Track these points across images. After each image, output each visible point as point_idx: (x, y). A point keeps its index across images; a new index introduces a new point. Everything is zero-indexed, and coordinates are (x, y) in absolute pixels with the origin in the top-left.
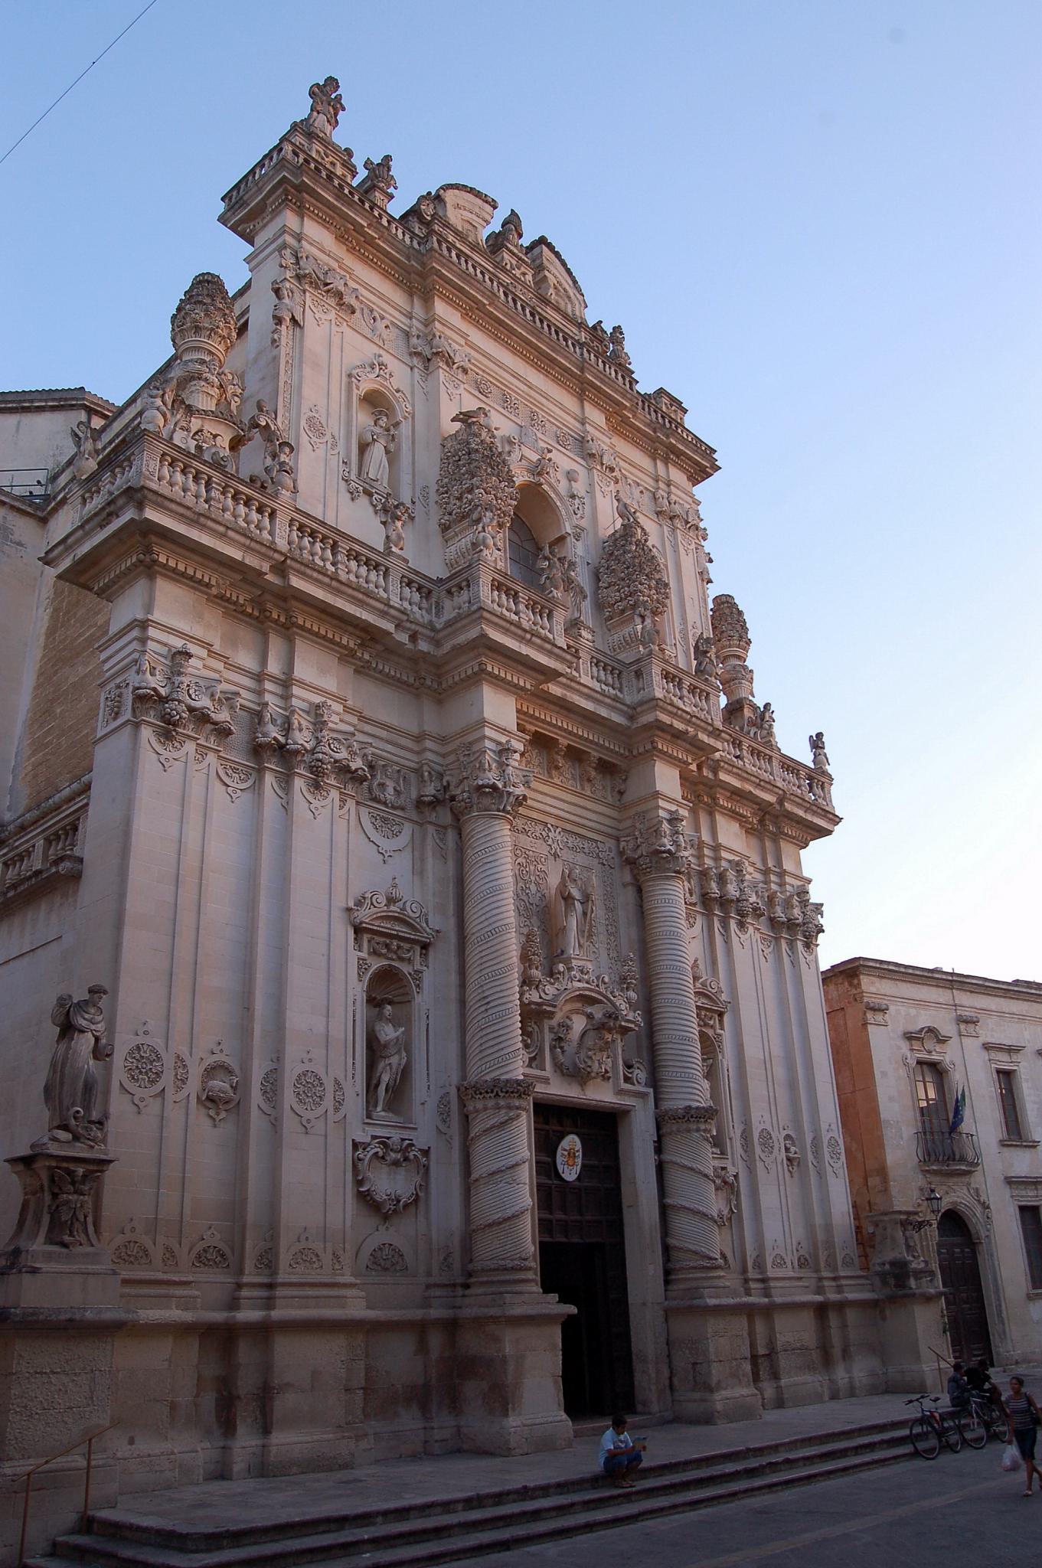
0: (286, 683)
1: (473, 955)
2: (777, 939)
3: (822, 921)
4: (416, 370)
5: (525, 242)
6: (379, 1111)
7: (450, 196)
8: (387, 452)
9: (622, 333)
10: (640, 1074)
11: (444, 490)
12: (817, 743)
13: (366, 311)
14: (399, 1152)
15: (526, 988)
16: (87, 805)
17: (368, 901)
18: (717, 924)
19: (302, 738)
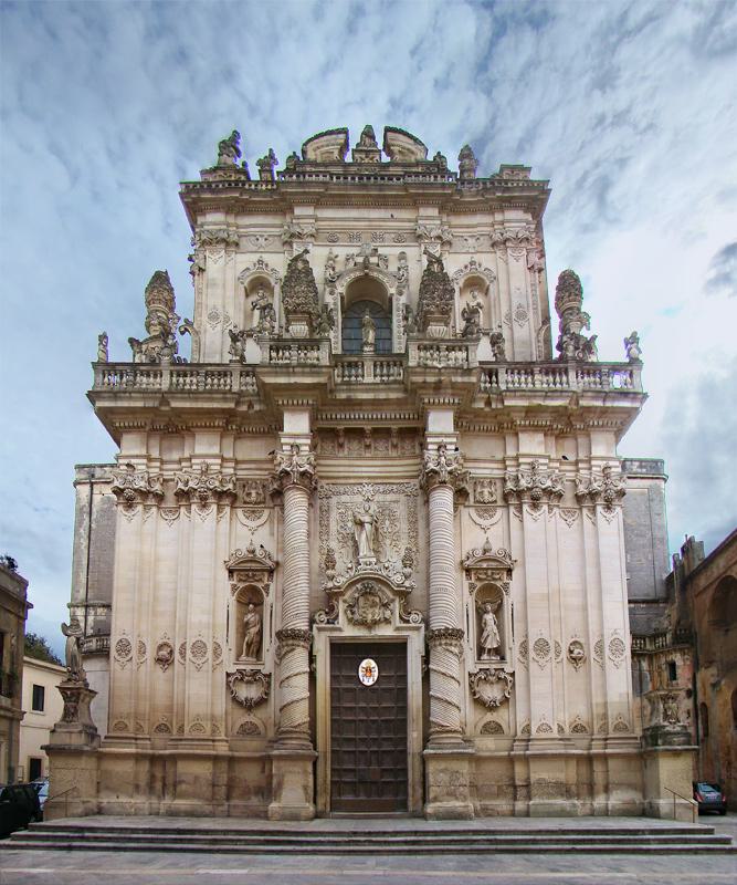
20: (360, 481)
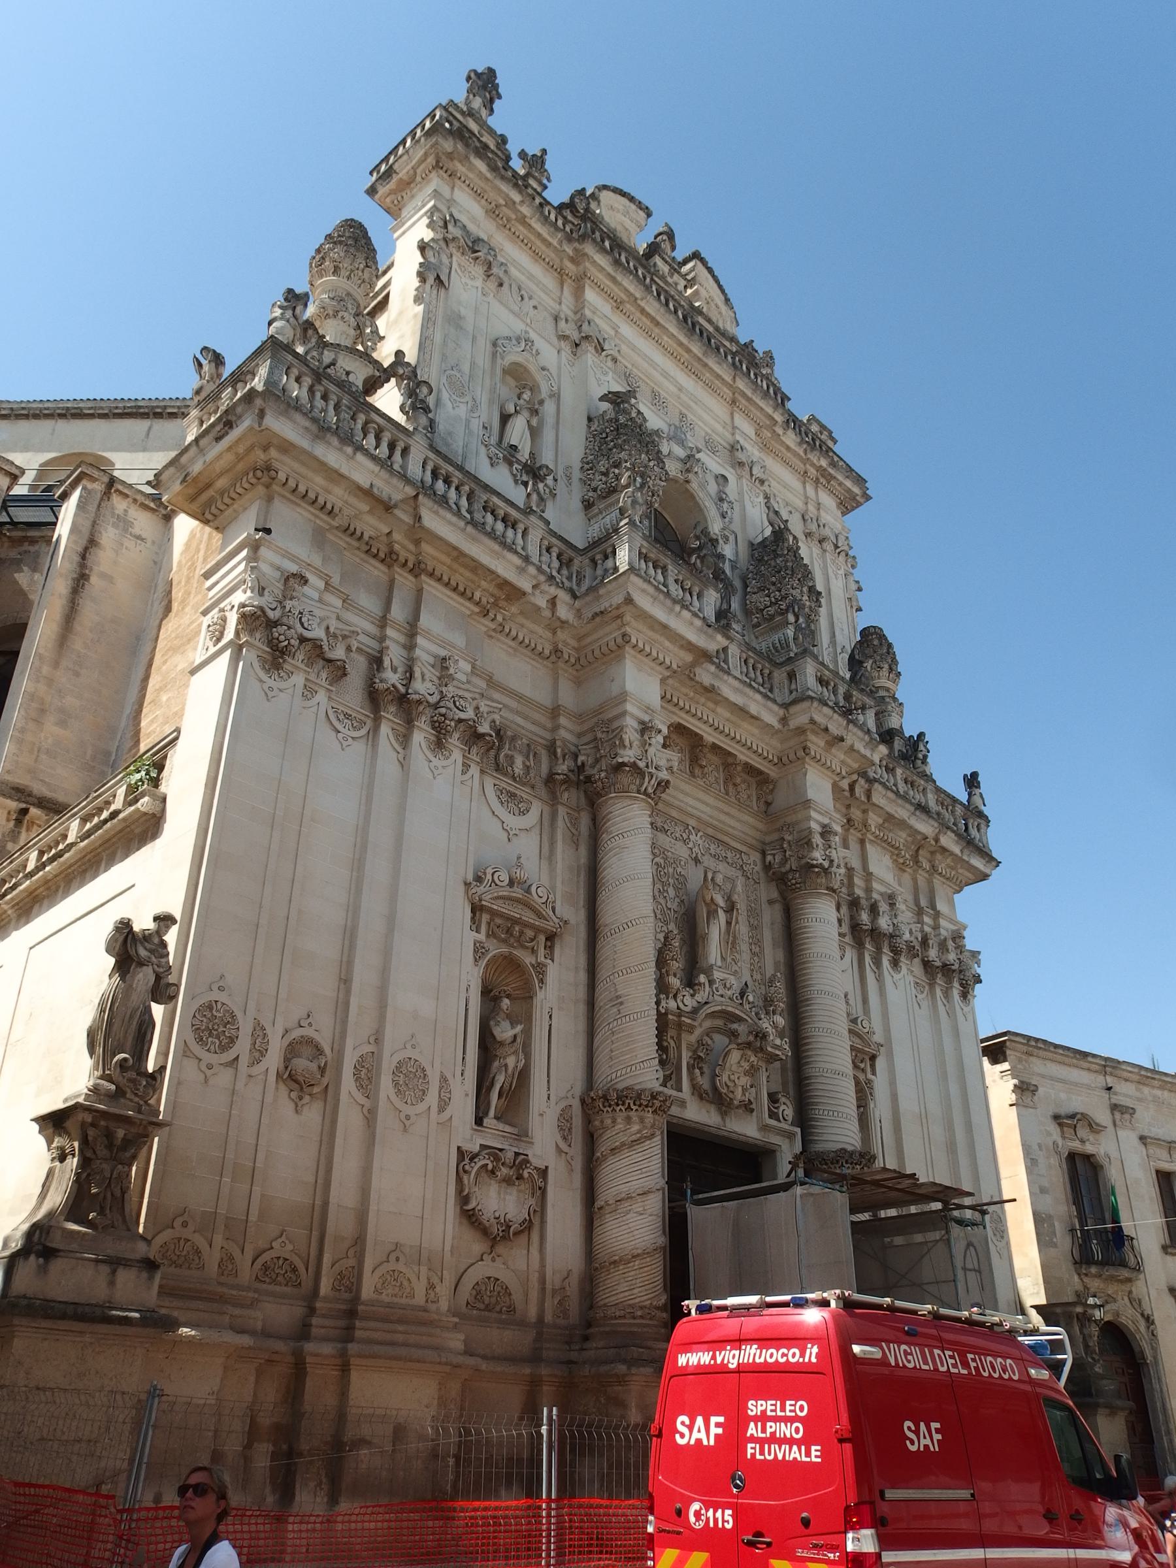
0: (412, 631)
1: (605, 951)
2: (932, 985)
3: (979, 971)
4: (563, 353)
5: (680, 255)
6: (489, 1121)
7: (605, 196)
8: (530, 427)
9: (772, 358)
10: (787, 1110)
11: (588, 466)
12: (972, 781)
13: (514, 287)
14: (511, 1168)
15: (662, 996)
16: (176, 738)
17: (489, 877)
18: (868, 959)
19: (422, 687)
20: (684, 818)
